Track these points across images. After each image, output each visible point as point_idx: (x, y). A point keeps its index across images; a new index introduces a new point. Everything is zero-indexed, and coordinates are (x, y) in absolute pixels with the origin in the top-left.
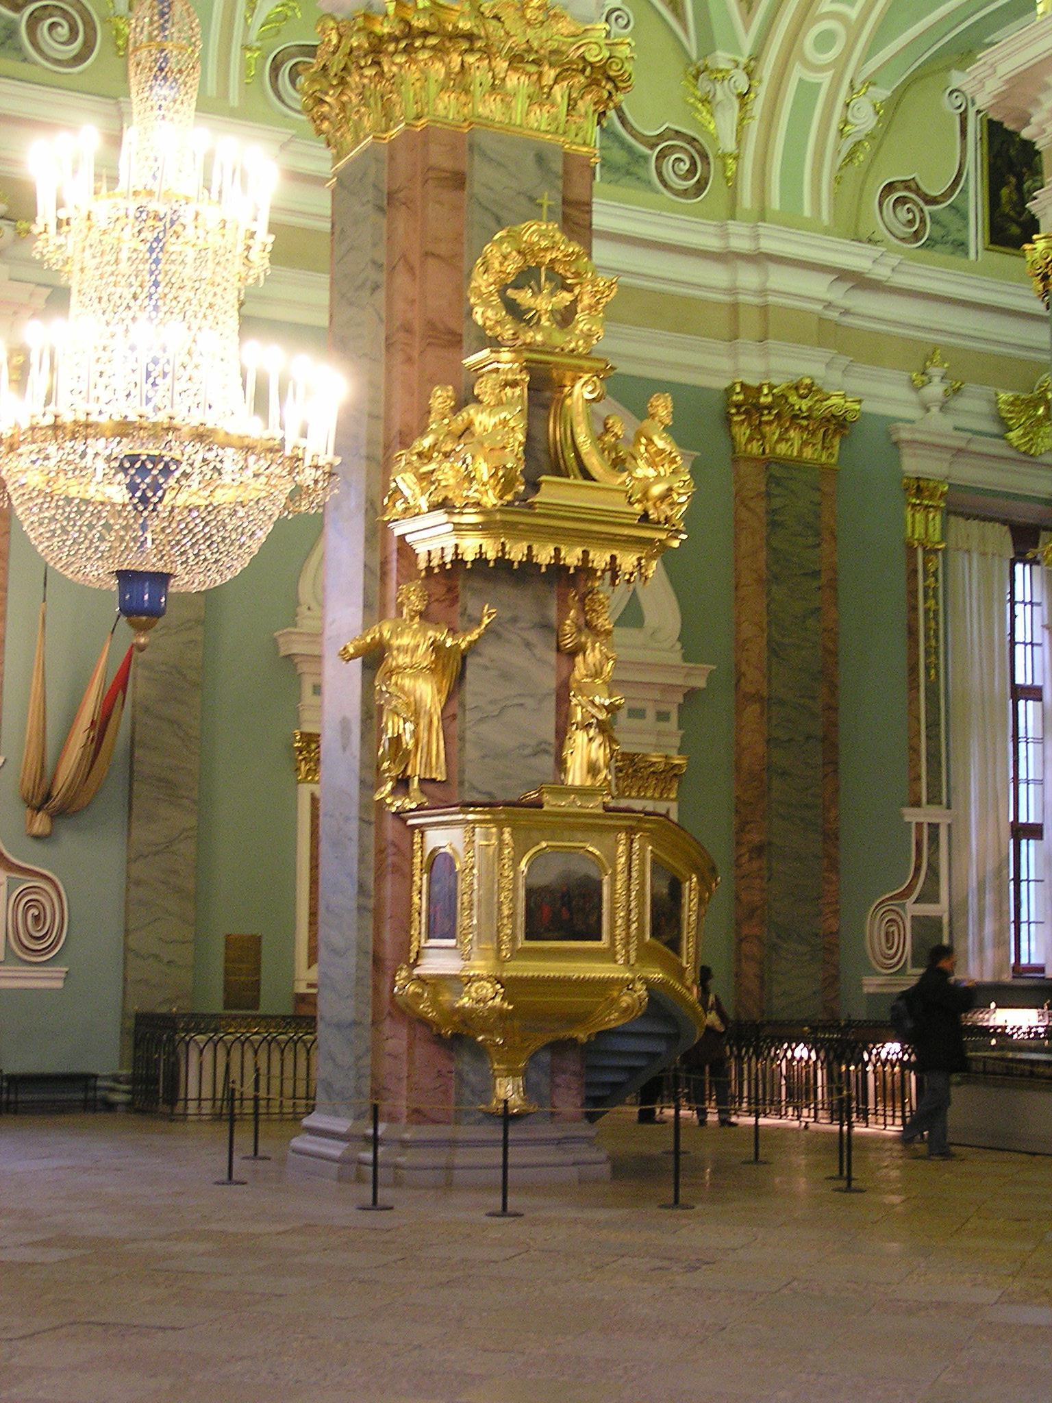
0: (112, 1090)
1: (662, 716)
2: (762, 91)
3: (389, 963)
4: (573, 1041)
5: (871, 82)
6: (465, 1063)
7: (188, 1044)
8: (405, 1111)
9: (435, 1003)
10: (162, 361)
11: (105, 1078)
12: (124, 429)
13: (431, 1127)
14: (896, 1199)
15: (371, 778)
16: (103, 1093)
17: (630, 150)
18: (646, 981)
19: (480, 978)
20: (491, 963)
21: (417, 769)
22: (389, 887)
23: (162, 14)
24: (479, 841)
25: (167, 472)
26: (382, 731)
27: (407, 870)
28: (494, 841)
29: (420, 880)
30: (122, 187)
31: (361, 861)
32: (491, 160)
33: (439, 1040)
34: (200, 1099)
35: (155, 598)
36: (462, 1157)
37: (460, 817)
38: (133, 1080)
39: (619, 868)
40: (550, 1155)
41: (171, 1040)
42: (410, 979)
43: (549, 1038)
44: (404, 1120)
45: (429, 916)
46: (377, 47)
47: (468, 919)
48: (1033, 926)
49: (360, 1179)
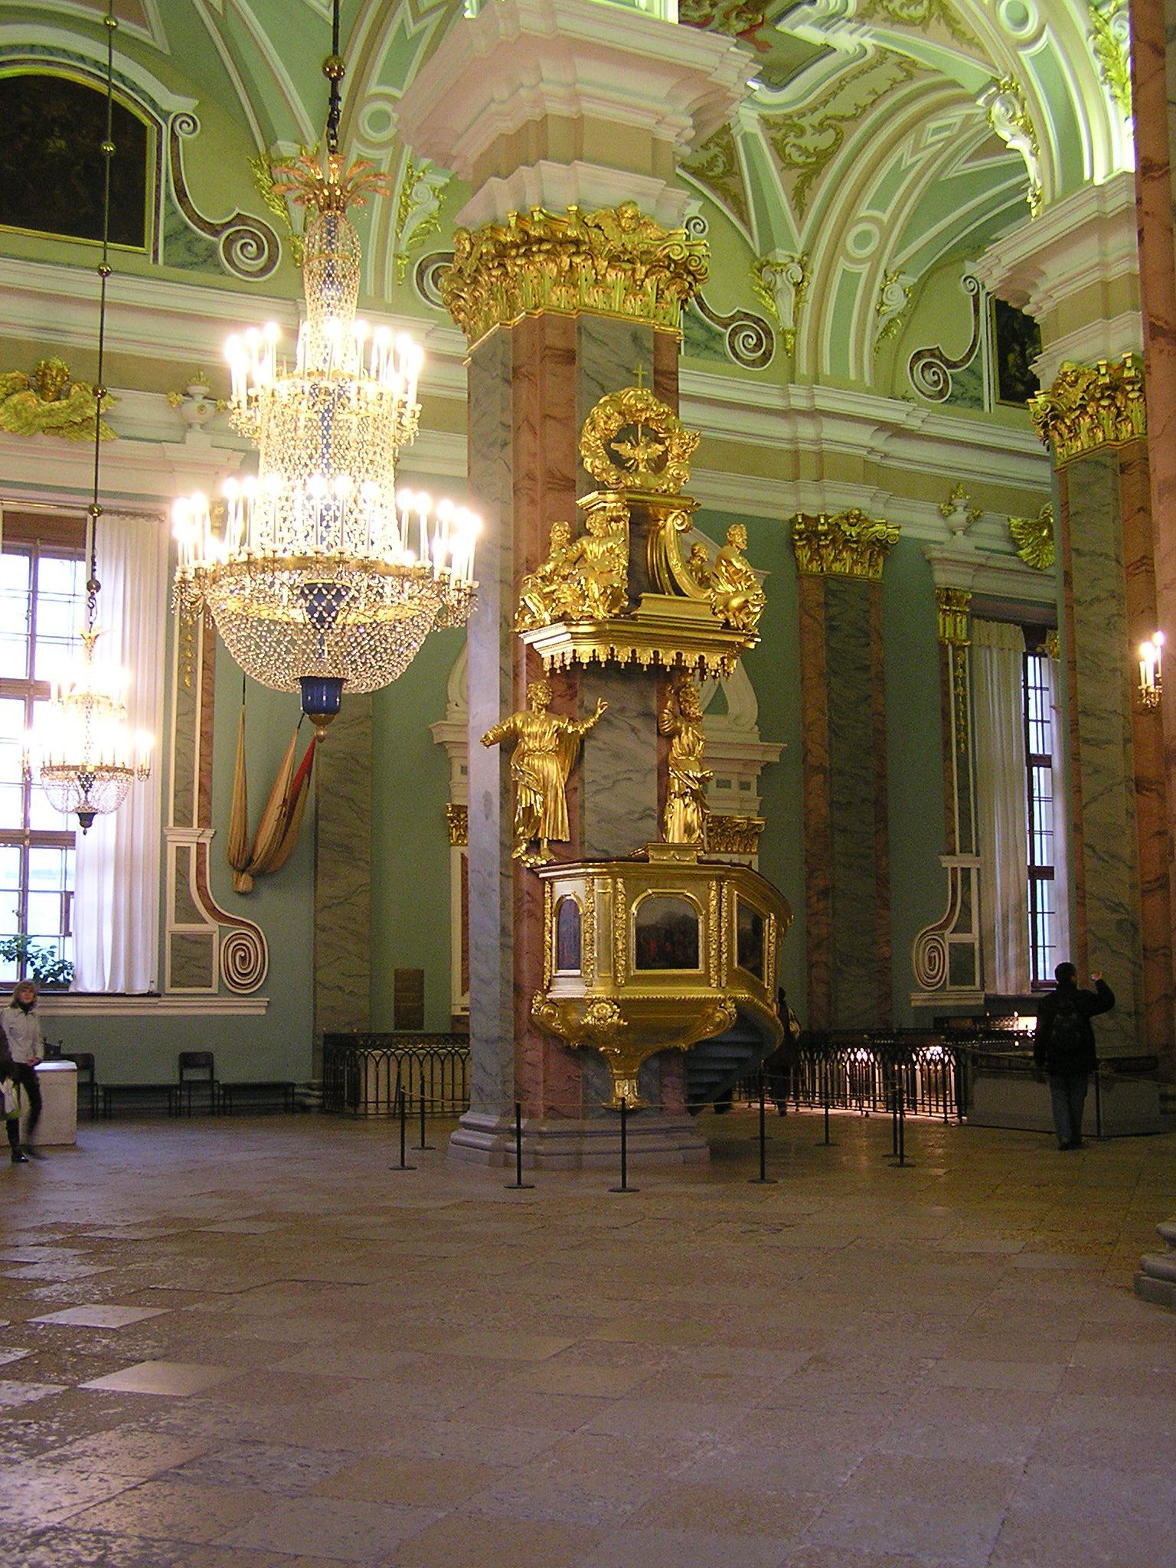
2: (814, 279)
3: (527, 990)
5: (901, 272)
7: (366, 1058)
9: (564, 1021)
10: (334, 508)
11: (301, 1086)
12: (304, 563)
13: (565, 1121)
14: (941, 1172)
16: (301, 1098)
17: (708, 329)
18: (735, 1000)
19: (600, 1000)
20: (610, 987)
21: (546, 833)
23: (329, 232)
24: (598, 890)
25: (339, 597)
26: (517, 802)
27: (539, 915)
29: (551, 922)
31: (503, 907)
32: (595, 340)
34: (377, 1102)
36: (587, 1145)
37: (582, 870)
38: (323, 1087)
39: (712, 909)
41: (353, 1054)
42: (544, 1002)
43: (657, 1048)
44: (542, 1116)
45: (558, 952)
46: (502, 253)
49: (507, 1164)
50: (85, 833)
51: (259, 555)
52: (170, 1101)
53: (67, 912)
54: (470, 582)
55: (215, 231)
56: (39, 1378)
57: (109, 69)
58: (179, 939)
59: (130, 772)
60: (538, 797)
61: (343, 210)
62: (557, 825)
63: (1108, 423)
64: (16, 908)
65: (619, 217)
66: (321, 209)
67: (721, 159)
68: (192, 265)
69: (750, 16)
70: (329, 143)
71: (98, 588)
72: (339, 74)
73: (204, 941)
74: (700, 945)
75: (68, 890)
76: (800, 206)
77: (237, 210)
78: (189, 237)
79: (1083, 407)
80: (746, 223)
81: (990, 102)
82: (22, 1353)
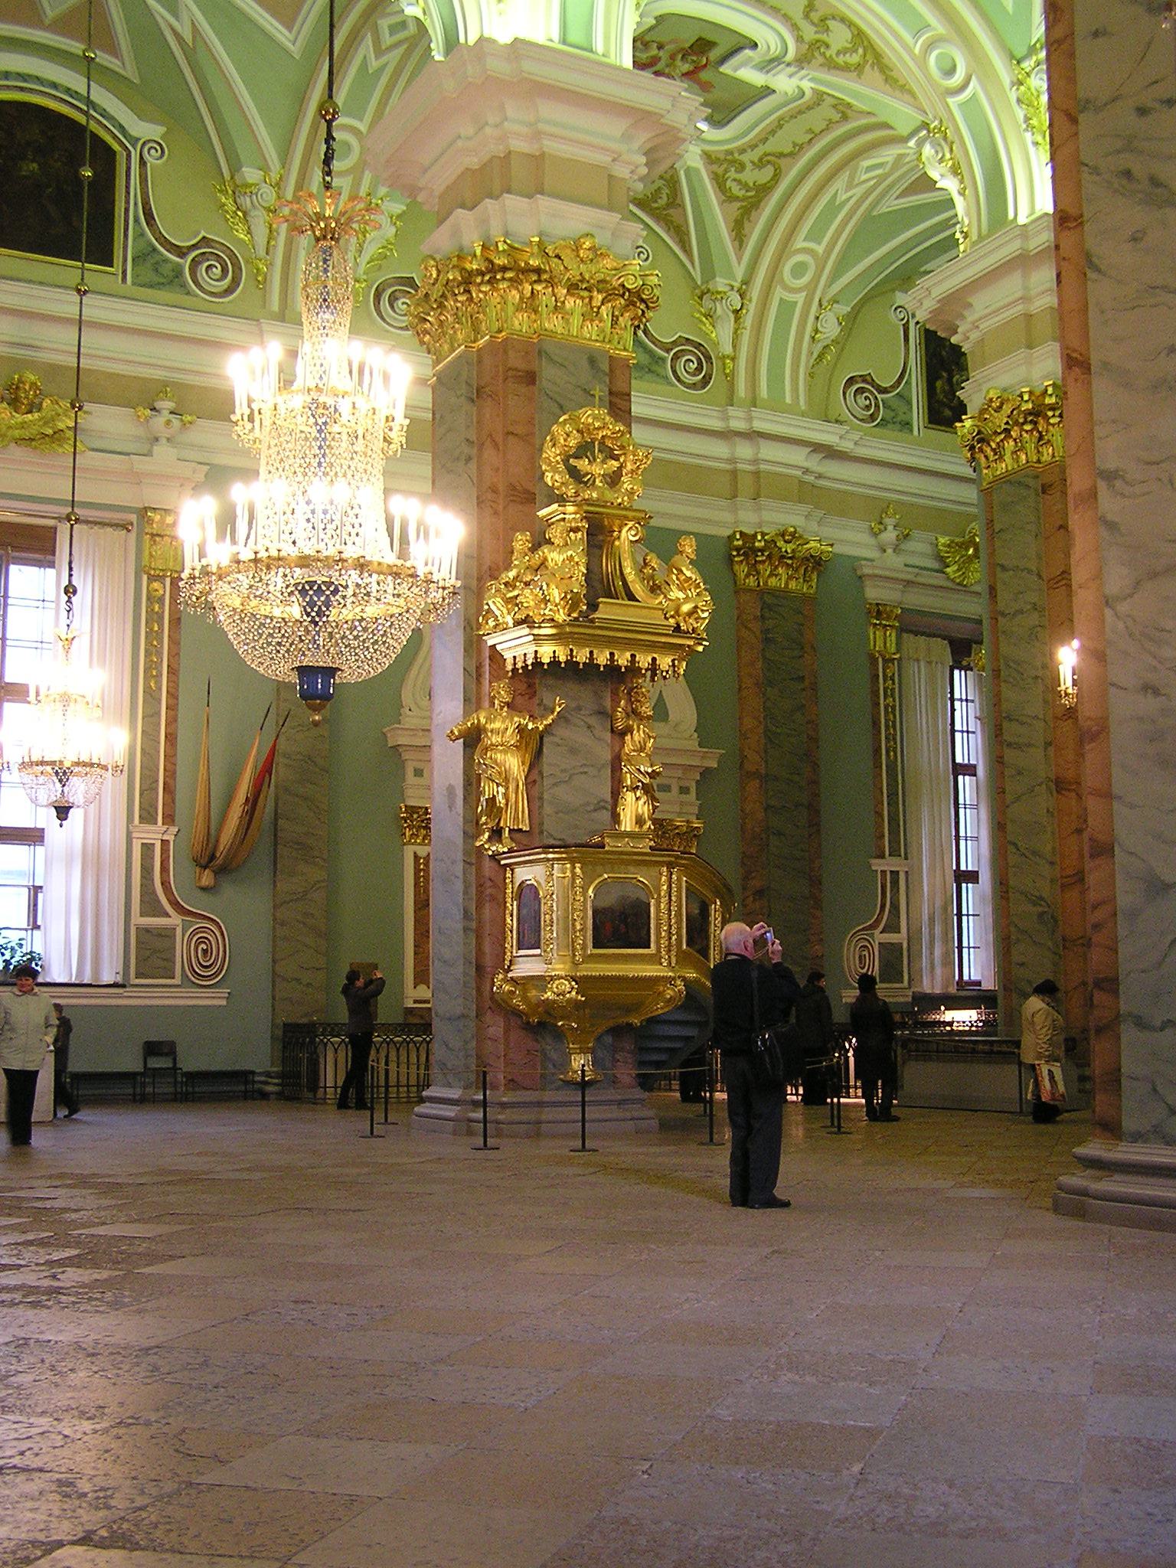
0: (266, 1083)
1: (684, 790)
2: (752, 308)
4: (629, 1025)
5: (835, 301)
6: (548, 1045)
7: (326, 1044)
8: (503, 1081)
10: (331, 512)
11: (260, 1074)
12: (304, 562)
15: (472, 830)
16: (260, 1085)
17: (650, 353)
18: (684, 979)
21: (507, 822)
22: (487, 912)
23: (325, 261)
24: (556, 873)
25: (336, 592)
28: (568, 874)
29: (512, 906)
30: (298, 385)
31: (466, 893)
32: (555, 362)
33: (528, 1027)
35: (326, 685)
36: (547, 1114)
37: (543, 856)
38: (282, 1075)
40: (614, 1112)
41: (312, 1042)
42: (505, 980)
43: (611, 1023)
45: (518, 933)
46: (467, 280)
47: (551, 933)
48: (971, 918)
49: (470, 1133)
50: (61, 826)
51: (263, 555)
52: (134, 1088)
53: (35, 905)
54: (453, 581)
55: (181, 252)
56: (96, 1265)
57: (89, 102)
58: (144, 932)
59: (105, 768)
60: (500, 788)
61: (337, 240)
62: (517, 814)
63: (1031, 447)
65: (577, 248)
66: (318, 240)
67: (666, 191)
68: (158, 286)
69: (695, 58)
70: (324, 179)
71: (75, 592)
72: (333, 116)
73: (168, 934)
74: (652, 926)
75: (36, 884)
76: (740, 238)
77: (203, 234)
78: (157, 258)
80: (687, 251)
81: (920, 144)
82: (75, 1252)
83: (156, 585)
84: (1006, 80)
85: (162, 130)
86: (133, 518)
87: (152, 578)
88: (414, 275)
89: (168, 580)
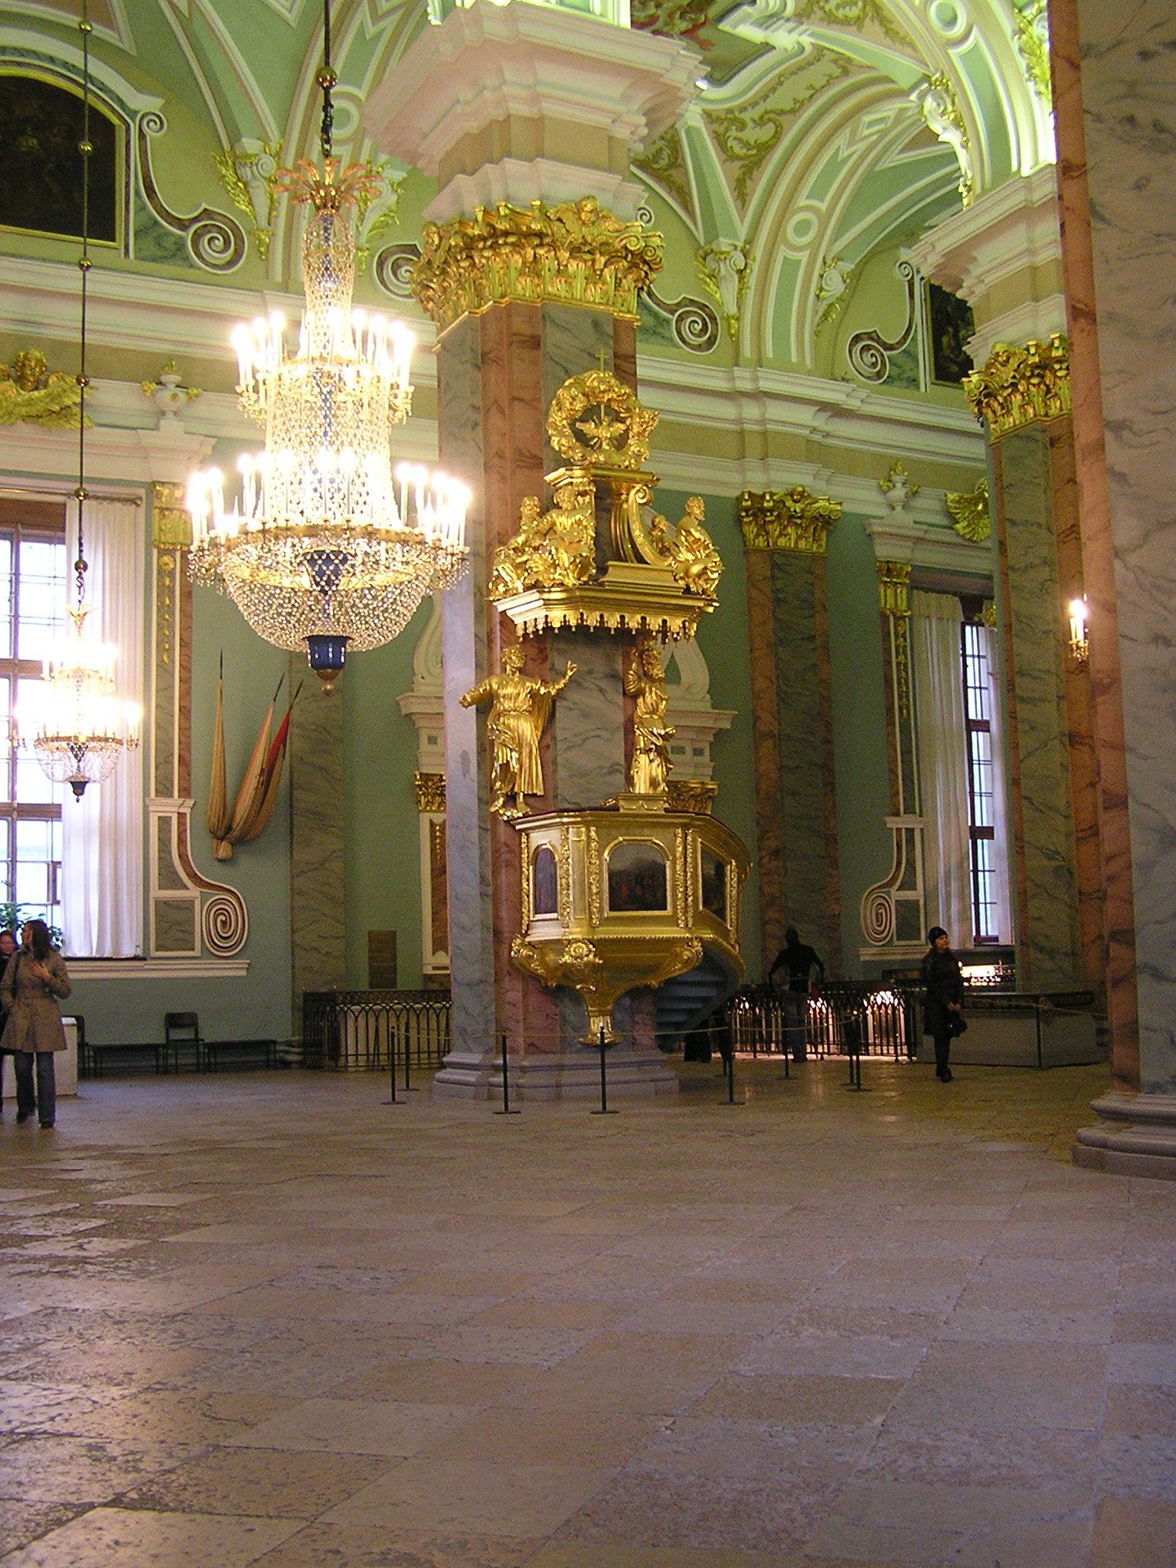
0: (287, 1052)
1: (698, 752)
2: (756, 267)
3: (506, 935)
4: (648, 987)
5: (839, 258)
6: (567, 1008)
7: (346, 1013)
8: (523, 1046)
9: (543, 963)
10: (337, 481)
11: (282, 1043)
12: (312, 531)
13: (542, 1056)
14: (893, 1094)
15: (486, 797)
17: (656, 315)
18: (701, 940)
19: (577, 941)
20: (585, 929)
21: (522, 787)
22: (504, 877)
23: (326, 230)
24: (572, 837)
25: (344, 561)
26: (494, 759)
27: (517, 864)
28: (584, 837)
29: (528, 871)
30: (302, 354)
31: (481, 859)
33: (546, 990)
34: (357, 1055)
35: (337, 654)
36: (566, 1077)
37: (558, 820)
39: (678, 855)
40: (633, 1074)
41: (333, 1010)
42: (523, 945)
43: (629, 986)
44: (522, 1052)
45: (535, 898)
46: (470, 246)
47: (567, 897)
48: (987, 874)
49: (491, 1098)
50: (78, 801)
51: (271, 525)
52: (157, 1061)
53: (55, 880)
54: (461, 547)
55: (183, 225)
56: (122, 1235)
57: (87, 76)
58: (163, 905)
59: (120, 742)
60: (514, 753)
61: (338, 209)
62: (531, 779)
63: (1038, 400)
64: (5, 878)
65: (579, 211)
66: (318, 208)
67: (666, 152)
68: (162, 259)
69: (693, 16)
70: (323, 147)
71: (85, 568)
72: (331, 83)
73: (187, 906)
74: (668, 887)
75: (55, 860)
76: (742, 195)
77: (204, 206)
79: (1014, 385)
80: (691, 213)
81: (922, 97)
82: (101, 1222)
83: (166, 559)
84: (1008, 29)
85: (160, 102)
86: (142, 492)
87: (162, 553)
88: (416, 243)
89: (178, 554)
